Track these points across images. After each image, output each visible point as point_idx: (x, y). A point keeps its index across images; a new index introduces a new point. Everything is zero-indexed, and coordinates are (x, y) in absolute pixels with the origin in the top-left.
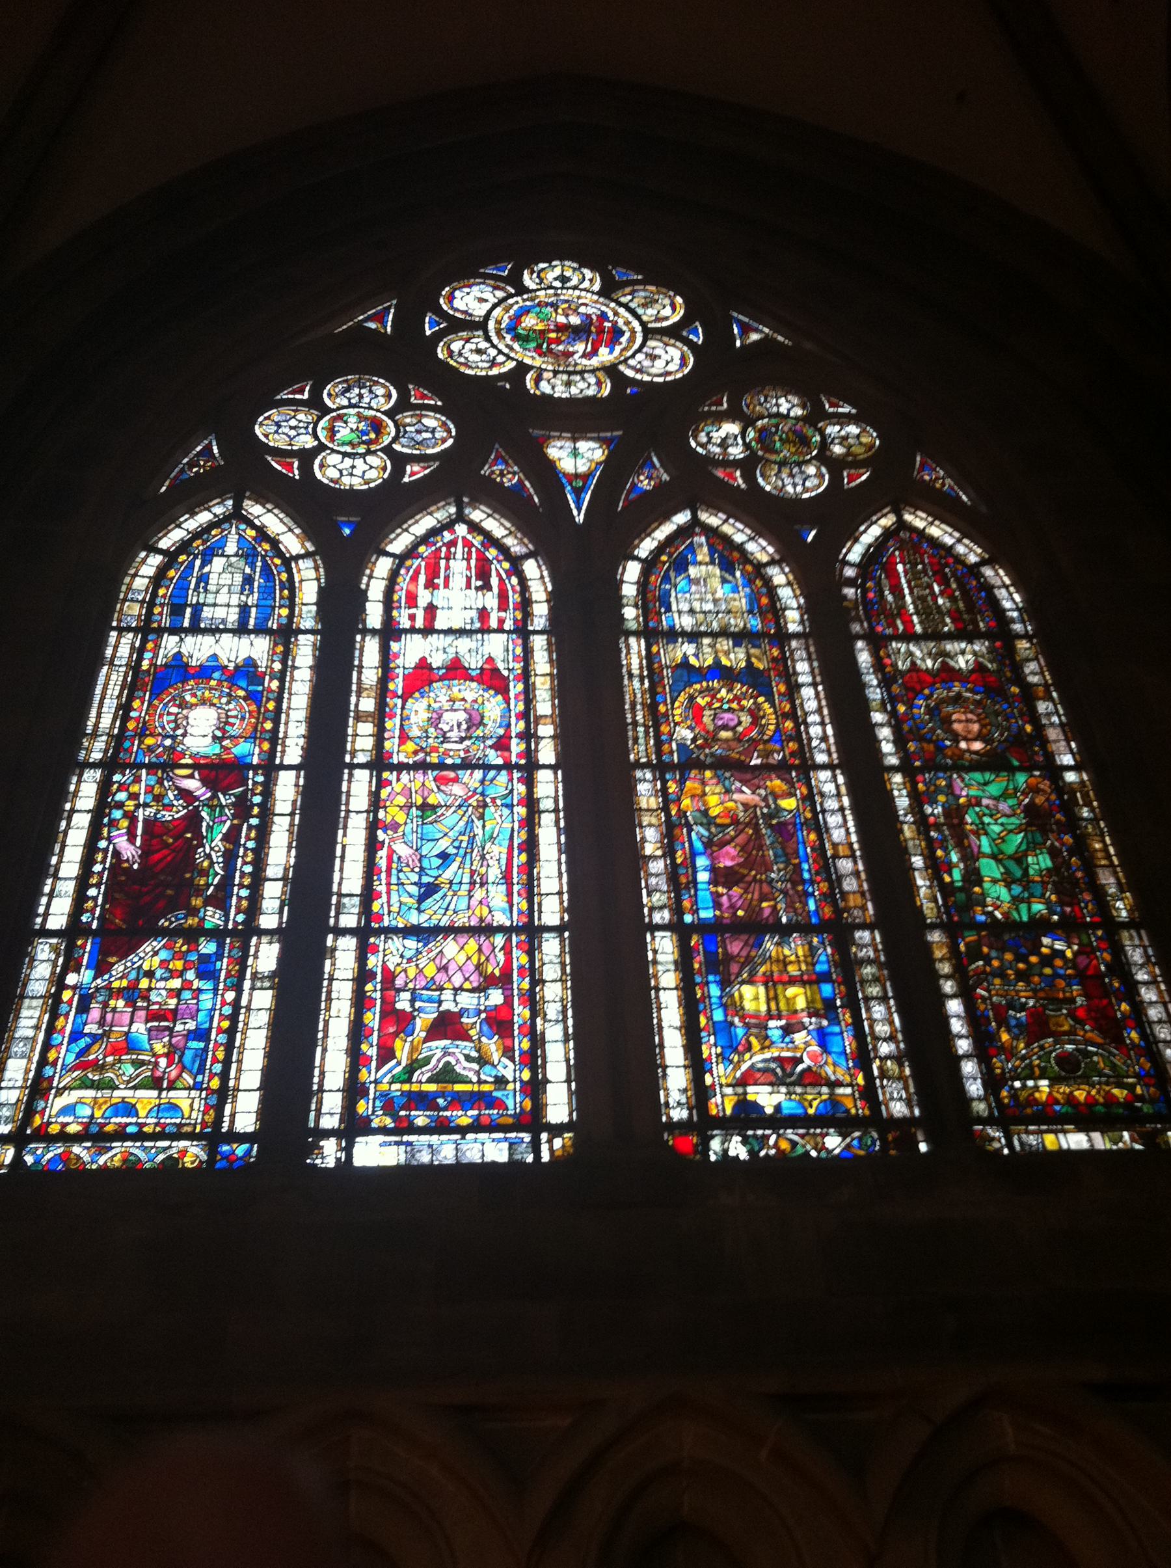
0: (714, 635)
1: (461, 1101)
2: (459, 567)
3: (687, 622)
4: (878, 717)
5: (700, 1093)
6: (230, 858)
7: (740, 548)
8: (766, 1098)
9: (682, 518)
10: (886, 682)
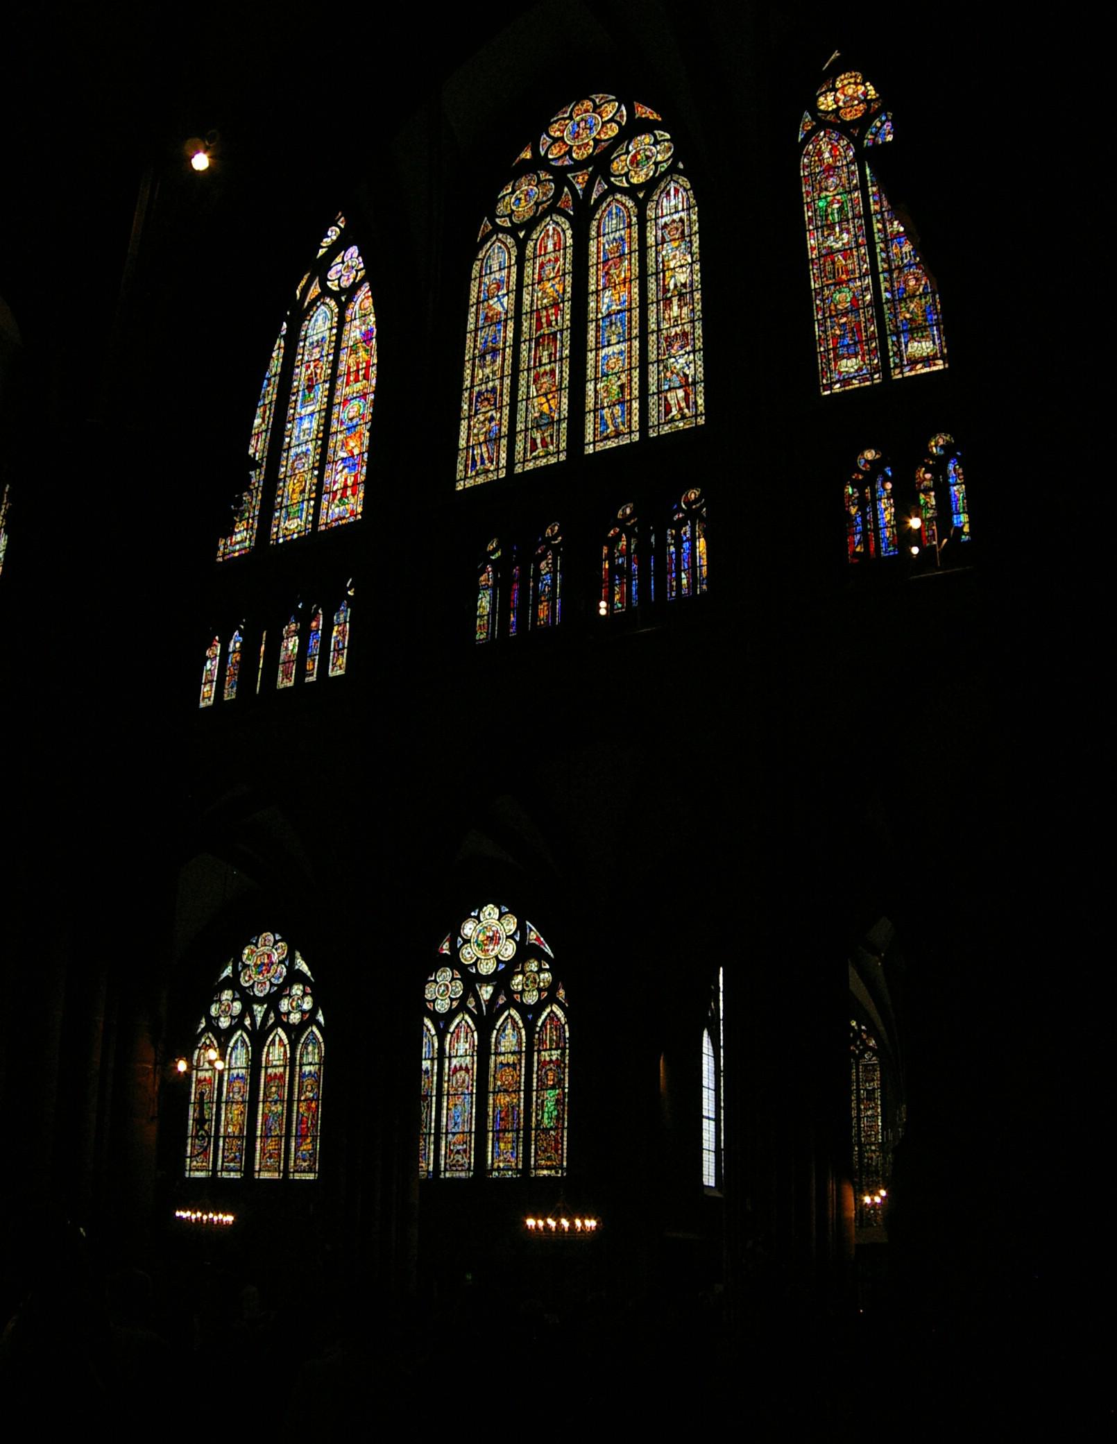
0: (507, 1053)
1: (460, 1166)
2: (462, 1035)
3: (503, 1049)
4: (535, 1076)
5: (493, 1163)
6: (426, 1117)
7: (517, 1023)
8: (502, 1165)
9: (506, 1013)
10: (538, 1064)
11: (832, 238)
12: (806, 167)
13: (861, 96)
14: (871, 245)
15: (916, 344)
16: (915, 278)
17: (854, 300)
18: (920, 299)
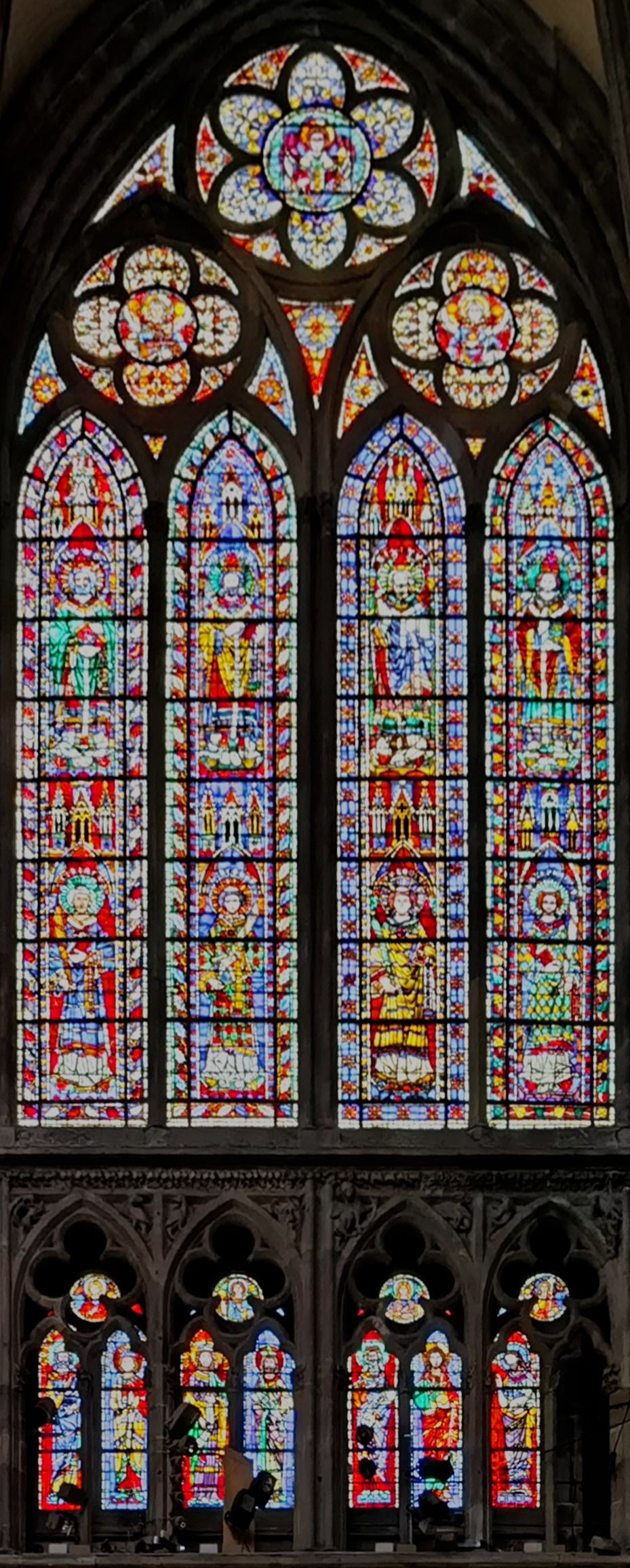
11: (70, 736)
12: (29, 514)
13: (179, 338)
14: (156, 780)
15: (223, 1056)
16: (241, 893)
17: (105, 915)
18: (246, 949)
